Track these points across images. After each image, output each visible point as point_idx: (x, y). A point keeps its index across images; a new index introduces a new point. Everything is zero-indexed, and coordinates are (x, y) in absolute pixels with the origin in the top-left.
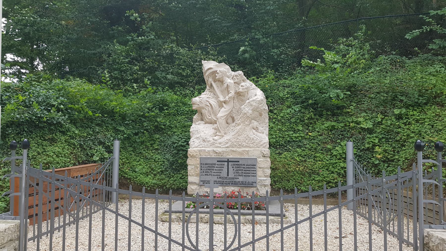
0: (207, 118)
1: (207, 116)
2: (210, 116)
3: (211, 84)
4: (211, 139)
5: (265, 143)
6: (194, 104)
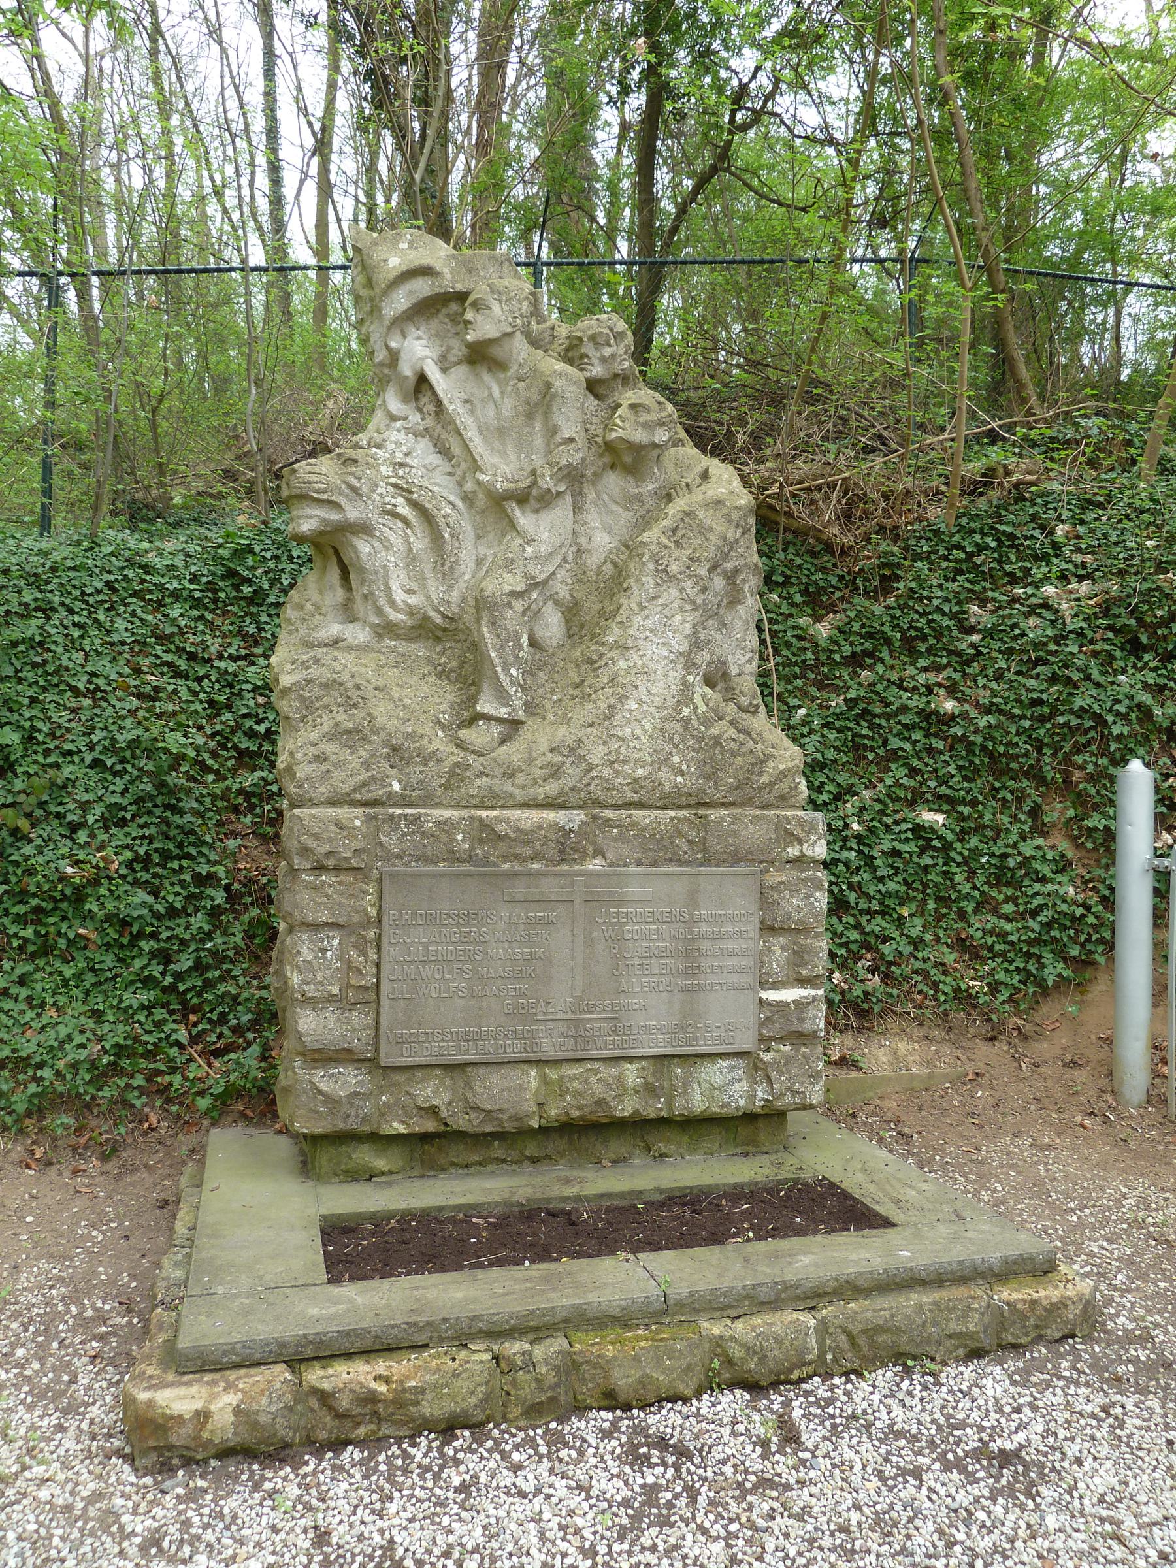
0: (392, 603)
1: (395, 587)
2: (410, 592)
3: (422, 380)
4: (439, 742)
5: (784, 774)
6: (303, 497)
